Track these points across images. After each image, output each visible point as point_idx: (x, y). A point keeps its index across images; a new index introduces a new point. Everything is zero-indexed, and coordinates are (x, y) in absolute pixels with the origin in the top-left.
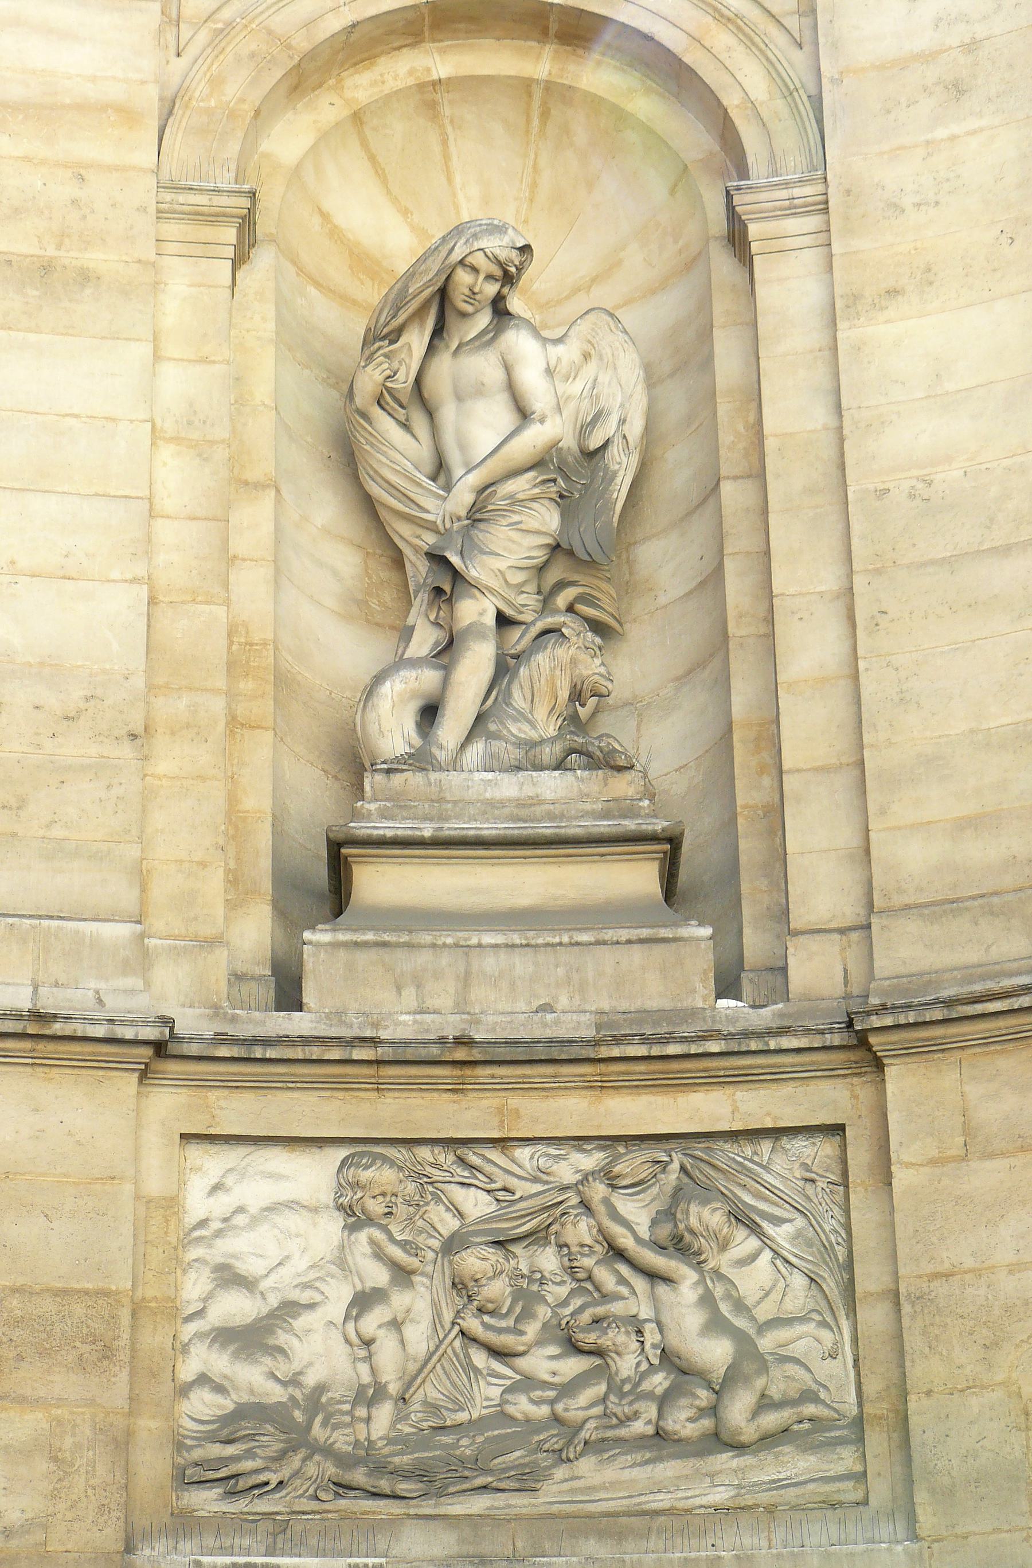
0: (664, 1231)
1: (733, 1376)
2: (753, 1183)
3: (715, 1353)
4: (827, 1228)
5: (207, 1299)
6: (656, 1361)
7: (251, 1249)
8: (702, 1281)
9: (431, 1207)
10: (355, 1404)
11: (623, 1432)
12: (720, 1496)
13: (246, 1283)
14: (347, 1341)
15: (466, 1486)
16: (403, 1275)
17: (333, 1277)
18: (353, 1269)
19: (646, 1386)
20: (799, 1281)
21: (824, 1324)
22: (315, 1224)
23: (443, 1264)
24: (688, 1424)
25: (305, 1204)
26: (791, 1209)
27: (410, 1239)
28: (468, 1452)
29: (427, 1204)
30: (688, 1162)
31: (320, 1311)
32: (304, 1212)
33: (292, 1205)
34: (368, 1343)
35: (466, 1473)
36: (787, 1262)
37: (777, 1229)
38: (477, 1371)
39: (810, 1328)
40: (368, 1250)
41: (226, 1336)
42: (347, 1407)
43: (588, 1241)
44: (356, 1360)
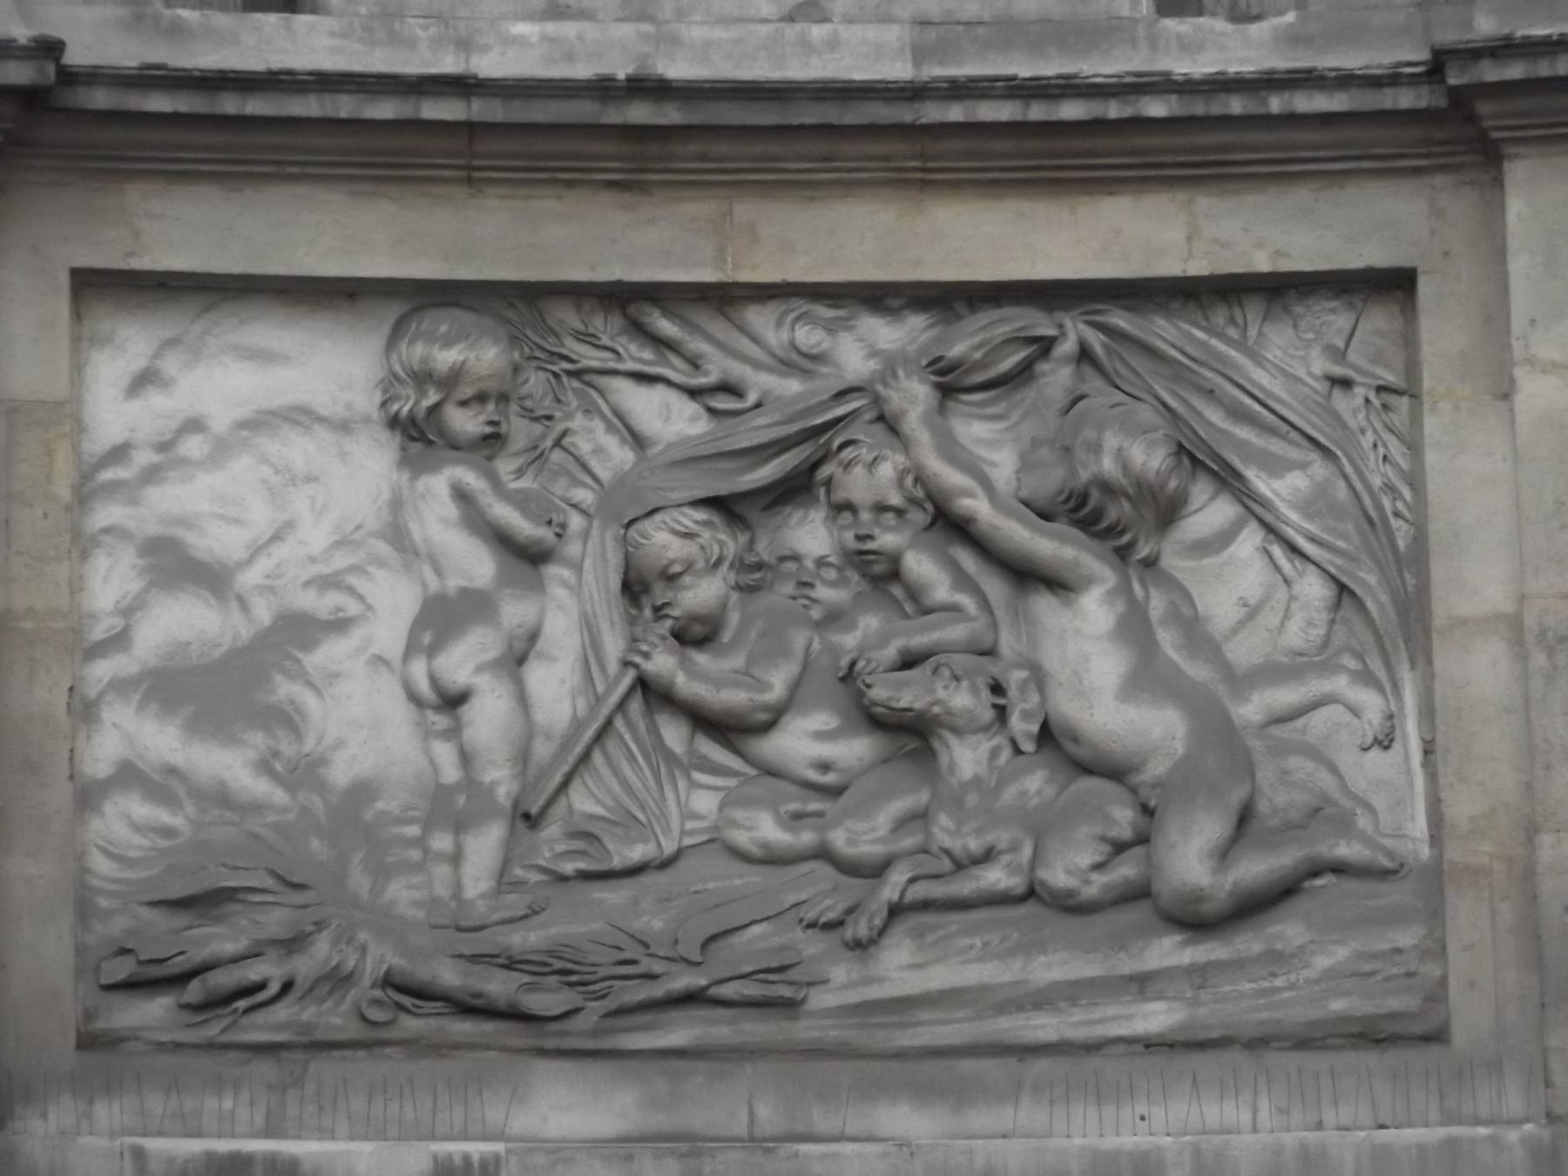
0: (1049, 481)
1: (1187, 782)
2: (1229, 388)
3: (1151, 730)
4: (1377, 481)
5: (130, 610)
6: (1028, 746)
7: (216, 505)
8: (1124, 589)
9: (578, 422)
10: (428, 825)
11: (964, 887)
12: (1155, 1017)
13: (210, 578)
14: (414, 698)
15: (658, 990)
16: (526, 558)
17: (381, 563)
18: (422, 548)
19: (1009, 794)
20: (1314, 589)
21: (1366, 677)
22: (343, 456)
23: (603, 544)
24: (1095, 876)
25: (324, 412)
26: (1305, 443)
27: (535, 486)
28: (657, 924)
29: (569, 416)
30: (1096, 340)
31: (356, 636)
32: (319, 430)
33: (300, 416)
34: (453, 701)
35: (657, 967)
36: (1293, 549)
37: (1277, 484)
38: (670, 757)
39: (1339, 684)
40: (451, 510)
41: (169, 686)
42: (413, 831)
43: (895, 499)
44: (427, 734)
